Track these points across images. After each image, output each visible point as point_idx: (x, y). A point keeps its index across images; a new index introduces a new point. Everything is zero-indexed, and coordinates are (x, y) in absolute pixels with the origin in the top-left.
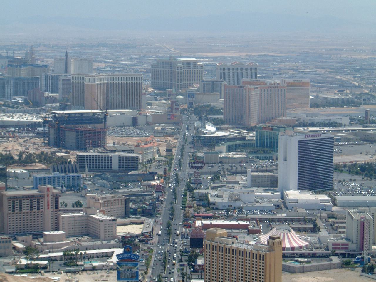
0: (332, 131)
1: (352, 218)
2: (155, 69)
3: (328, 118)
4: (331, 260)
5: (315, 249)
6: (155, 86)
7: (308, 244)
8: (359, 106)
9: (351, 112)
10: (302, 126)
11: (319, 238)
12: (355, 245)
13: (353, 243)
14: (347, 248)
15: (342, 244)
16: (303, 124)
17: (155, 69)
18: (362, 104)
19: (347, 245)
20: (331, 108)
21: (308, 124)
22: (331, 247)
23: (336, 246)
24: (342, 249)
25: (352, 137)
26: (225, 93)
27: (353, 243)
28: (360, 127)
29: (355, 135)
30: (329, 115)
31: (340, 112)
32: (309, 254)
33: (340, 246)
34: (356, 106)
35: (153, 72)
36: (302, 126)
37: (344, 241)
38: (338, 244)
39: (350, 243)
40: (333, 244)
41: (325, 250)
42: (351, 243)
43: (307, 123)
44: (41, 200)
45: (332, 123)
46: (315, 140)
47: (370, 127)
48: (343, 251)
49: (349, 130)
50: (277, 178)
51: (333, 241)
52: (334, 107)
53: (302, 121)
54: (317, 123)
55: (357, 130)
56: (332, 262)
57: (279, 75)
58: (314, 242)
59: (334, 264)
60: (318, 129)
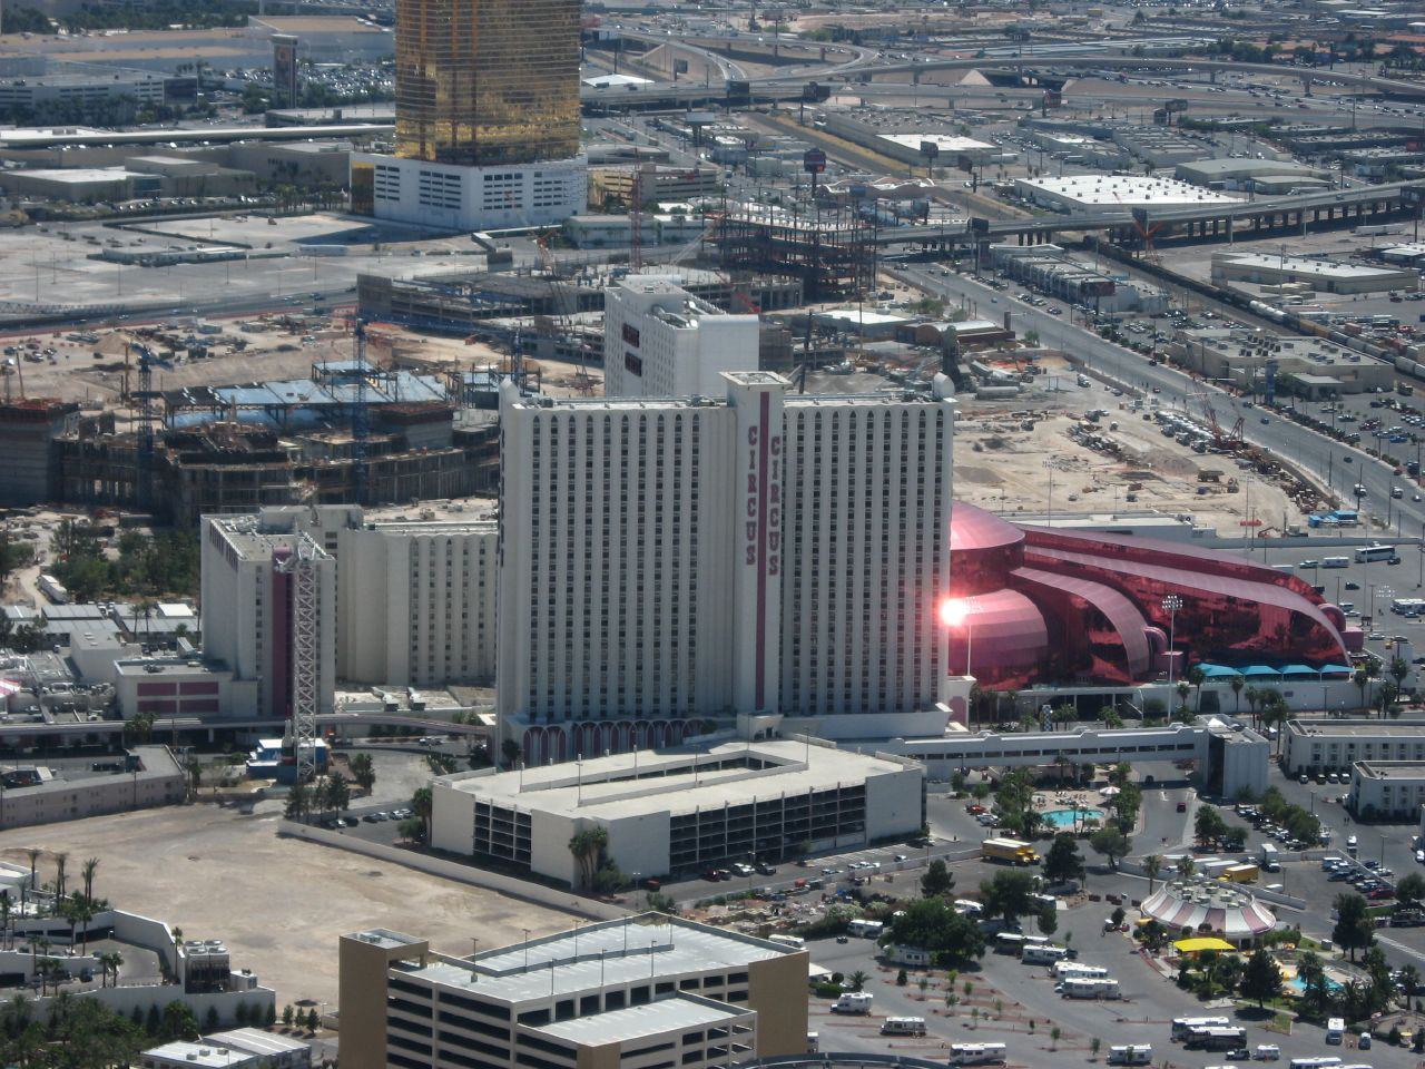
0: (117, 143)
1: (232, 555)
3: (95, 81)
4: (134, 765)
5: (53, 711)
7: (17, 688)
8: (245, 23)
9: (206, 52)
11: (70, 662)
12: (253, 687)
13: (238, 677)
14: (214, 705)
15: (189, 687)
18: (255, 13)
19: (213, 687)
20: (109, 33)
22: (130, 700)
23: (156, 696)
24: (189, 708)
25: (215, 171)
27: (238, 677)
28: (255, 123)
29: (228, 160)
30: (100, 67)
31: (150, 54)
32: (26, 739)
33: (178, 698)
34: (229, 23)
37: (196, 671)
38: (168, 688)
39: (224, 679)
40: (144, 688)
41: (106, 717)
42: (229, 675)
45: (114, 103)
47: (300, 122)
48: (192, 721)
49: (197, 140)
51: (140, 671)
54: (39, 105)
55: (238, 138)
56: (140, 776)
58: (49, 680)
59: (152, 783)
60: (47, 134)
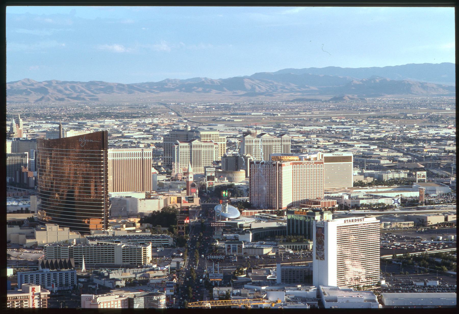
2: (168, 143)
6: (168, 163)
10: (343, 208)
16: (345, 205)
17: (168, 143)
21: (350, 207)
26: (250, 170)
35: (166, 146)
36: (343, 208)
43: (349, 205)
44: (25, 302)
46: (357, 225)
50: (312, 271)
52: (436, 262)
53: (343, 203)
57: (316, 148)
